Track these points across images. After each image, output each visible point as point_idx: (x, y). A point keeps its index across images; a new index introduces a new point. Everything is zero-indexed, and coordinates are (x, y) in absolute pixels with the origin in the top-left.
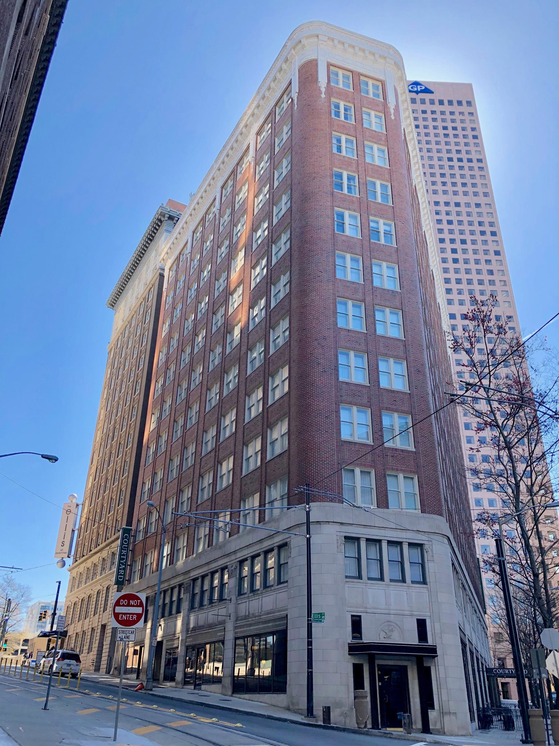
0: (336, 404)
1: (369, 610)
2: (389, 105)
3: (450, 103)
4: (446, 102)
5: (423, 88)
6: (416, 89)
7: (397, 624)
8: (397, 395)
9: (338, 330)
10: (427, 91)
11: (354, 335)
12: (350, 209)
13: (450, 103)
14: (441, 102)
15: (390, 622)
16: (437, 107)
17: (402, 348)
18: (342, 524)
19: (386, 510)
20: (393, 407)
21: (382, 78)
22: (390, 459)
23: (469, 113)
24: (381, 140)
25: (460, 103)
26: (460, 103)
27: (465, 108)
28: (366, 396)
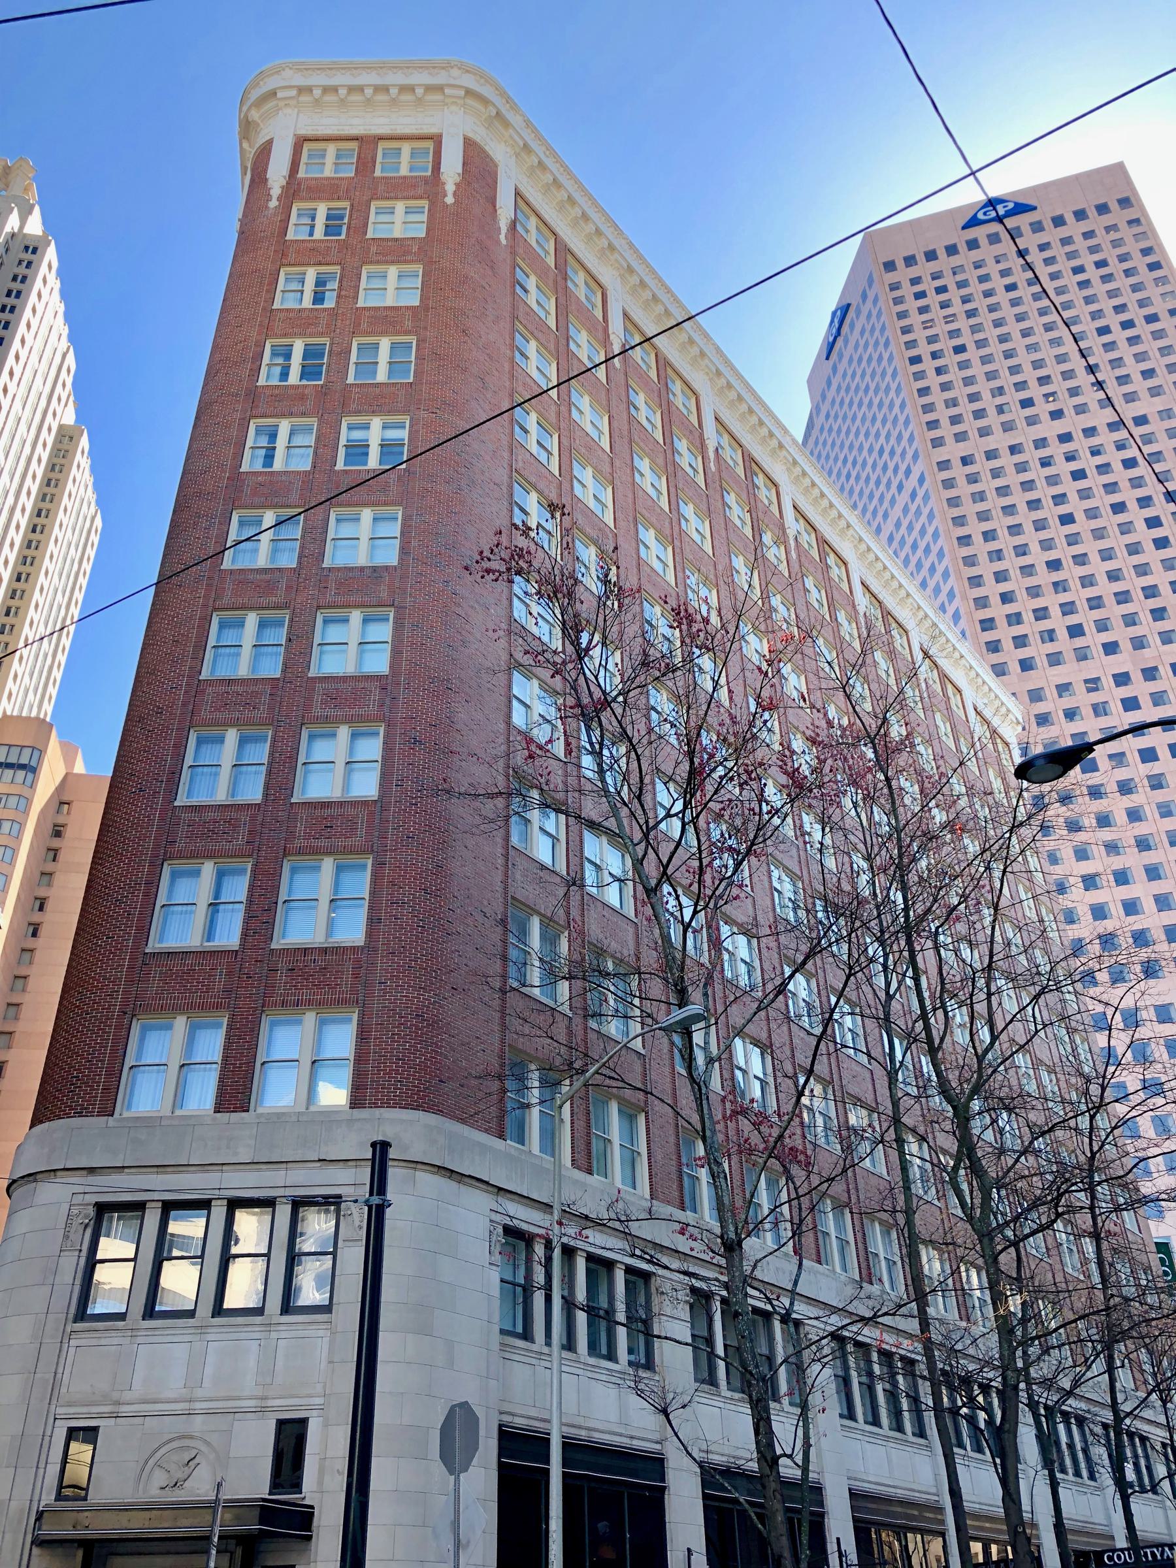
0: (152, 864)
1: (125, 1409)
2: (443, 177)
3: (1080, 215)
4: (1070, 218)
5: (1011, 205)
6: (993, 214)
7: (208, 1443)
8: (334, 811)
9: (199, 687)
10: (1021, 208)
11: (240, 689)
12: (291, 415)
13: (1080, 215)
14: (1059, 221)
15: (192, 1437)
16: (1052, 235)
17: (376, 695)
18: (91, 1170)
19: (235, 1117)
20: (323, 843)
21: (433, 130)
22: (281, 977)
23: (1130, 222)
24: (409, 252)
25: (1102, 209)
26: (1102, 209)
27: (1117, 216)
28: (243, 832)
